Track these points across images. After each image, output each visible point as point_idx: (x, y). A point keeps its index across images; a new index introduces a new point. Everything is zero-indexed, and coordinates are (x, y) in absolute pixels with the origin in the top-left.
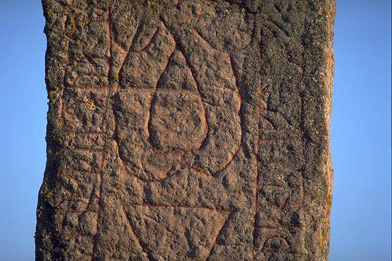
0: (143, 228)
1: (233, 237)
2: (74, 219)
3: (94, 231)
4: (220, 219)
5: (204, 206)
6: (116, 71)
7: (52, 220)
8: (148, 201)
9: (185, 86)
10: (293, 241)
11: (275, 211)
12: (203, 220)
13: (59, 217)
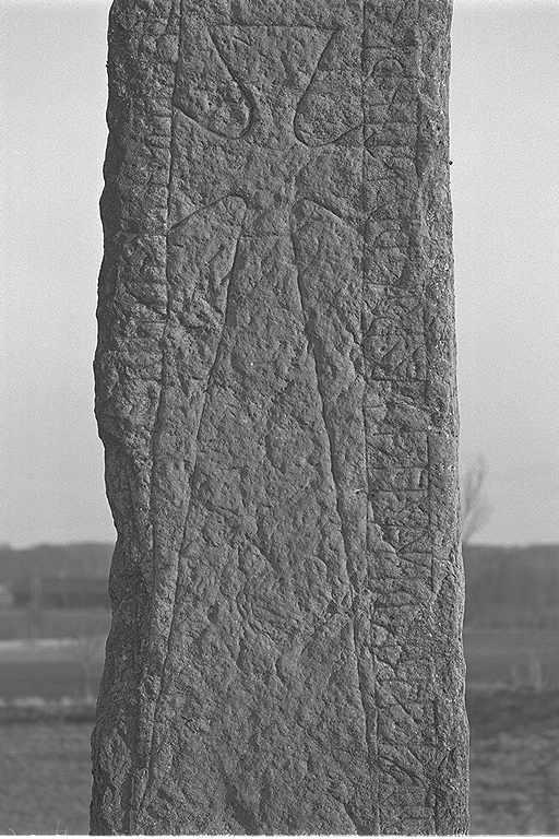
0: (233, 53)
1: (337, 61)
2: (151, 44)
3: (175, 57)
4: (322, 39)
5: (303, 24)
7: (126, 45)
8: (237, 20)
10: (407, 63)
11: (386, 28)
12: (302, 42)
13: (134, 42)
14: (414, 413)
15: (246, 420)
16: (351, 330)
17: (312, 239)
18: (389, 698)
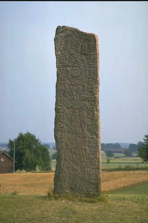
6: (66, 65)
9: (77, 67)
14: (95, 137)
15: (73, 137)
16: (86, 125)
17: (81, 113)
18: (91, 174)
